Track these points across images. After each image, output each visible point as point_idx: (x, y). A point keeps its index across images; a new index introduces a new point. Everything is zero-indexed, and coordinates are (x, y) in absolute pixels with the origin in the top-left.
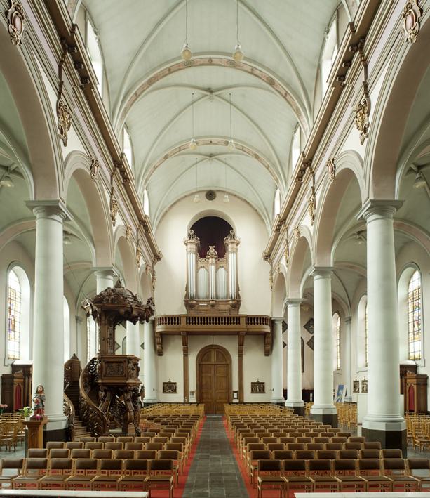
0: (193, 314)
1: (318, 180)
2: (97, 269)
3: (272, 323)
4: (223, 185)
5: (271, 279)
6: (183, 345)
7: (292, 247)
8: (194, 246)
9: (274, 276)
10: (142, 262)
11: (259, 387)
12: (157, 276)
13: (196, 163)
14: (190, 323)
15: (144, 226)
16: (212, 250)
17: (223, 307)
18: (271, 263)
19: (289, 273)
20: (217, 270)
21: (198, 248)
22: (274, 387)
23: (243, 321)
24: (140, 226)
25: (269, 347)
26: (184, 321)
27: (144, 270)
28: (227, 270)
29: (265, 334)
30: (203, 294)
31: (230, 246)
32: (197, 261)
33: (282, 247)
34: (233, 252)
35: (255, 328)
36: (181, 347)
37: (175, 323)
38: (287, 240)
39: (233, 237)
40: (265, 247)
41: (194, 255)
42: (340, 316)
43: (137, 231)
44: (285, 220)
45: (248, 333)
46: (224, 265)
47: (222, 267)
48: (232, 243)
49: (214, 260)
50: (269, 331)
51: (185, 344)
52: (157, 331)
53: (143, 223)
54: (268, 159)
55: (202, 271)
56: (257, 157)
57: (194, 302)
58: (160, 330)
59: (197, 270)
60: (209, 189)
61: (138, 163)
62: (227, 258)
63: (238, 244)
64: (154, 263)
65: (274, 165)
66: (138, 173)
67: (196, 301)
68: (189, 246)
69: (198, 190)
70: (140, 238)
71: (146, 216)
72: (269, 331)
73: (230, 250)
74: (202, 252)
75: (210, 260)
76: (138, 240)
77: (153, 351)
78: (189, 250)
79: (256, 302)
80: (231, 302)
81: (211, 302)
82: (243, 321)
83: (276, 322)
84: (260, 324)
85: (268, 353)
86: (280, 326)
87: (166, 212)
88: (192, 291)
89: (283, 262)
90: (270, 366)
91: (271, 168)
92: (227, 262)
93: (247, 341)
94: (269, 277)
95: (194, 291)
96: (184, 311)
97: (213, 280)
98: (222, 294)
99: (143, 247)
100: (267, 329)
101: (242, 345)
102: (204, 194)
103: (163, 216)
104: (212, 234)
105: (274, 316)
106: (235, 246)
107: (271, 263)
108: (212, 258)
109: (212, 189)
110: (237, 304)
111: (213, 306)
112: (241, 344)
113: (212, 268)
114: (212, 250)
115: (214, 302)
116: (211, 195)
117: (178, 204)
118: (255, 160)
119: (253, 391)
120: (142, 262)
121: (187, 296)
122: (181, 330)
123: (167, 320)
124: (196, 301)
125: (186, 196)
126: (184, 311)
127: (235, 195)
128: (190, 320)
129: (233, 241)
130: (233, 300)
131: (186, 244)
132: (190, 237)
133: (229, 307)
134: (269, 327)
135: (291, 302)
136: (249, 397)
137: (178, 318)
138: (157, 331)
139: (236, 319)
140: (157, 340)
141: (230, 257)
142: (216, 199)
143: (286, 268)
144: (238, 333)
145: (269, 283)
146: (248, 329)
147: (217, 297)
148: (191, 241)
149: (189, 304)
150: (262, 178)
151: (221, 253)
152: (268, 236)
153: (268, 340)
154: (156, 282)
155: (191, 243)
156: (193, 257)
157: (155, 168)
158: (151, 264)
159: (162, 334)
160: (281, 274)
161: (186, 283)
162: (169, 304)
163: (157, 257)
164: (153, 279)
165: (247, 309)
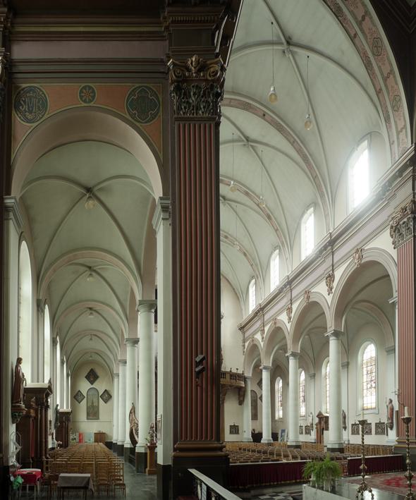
3: (245, 379)
11: (235, 430)
19: (265, 349)
22: (245, 429)
23: (228, 376)
25: (242, 399)
29: (242, 387)
56: (245, 255)
65: (256, 265)
82: (228, 376)
85: (241, 403)
90: (242, 414)
91: (254, 266)
118: (244, 257)
119: (231, 433)
136: (228, 437)
153: (242, 393)
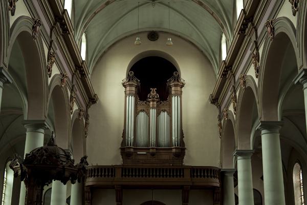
2: (28, 122)
3: (222, 175)
4: (166, 26)
6: (117, 201)
7: (224, 122)
8: (134, 89)
9: (222, 122)
10: (75, 108)
13: (139, 6)
15: (80, 72)
16: (153, 92)
17: (165, 156)
18: (219, 107)
20: (158, 114)
21: (138, 90)
23: (187, 173)
24: (75, 71)
26: (118, 173)
27: (77, 116)
28: (170, 114)
29: (215, 187)
31: (173, 88)
33: (229, 93)
34: (176, 95)
37: (108, 175)
38: (234, 87)
39: (178, 78)
40: (212, 90)
42: (301, 168)
43: (73, 76)
44: (231, 66)
45: (194, 187)
47: (164, 111)
48: (176, 86)
49: (155, 103)
50: (218, 185)
52: (87, 184)
53: (79, 68)
54: (212, 6)
55: (142, 115)
58: (90, 184)
59: (136, 113)
60: (151, 30)
61: (78, 11)
62: (171, 101)
63: (182, 86)
64: (88, 106)
65: (218, 12)
66: (77, 19)
68: (128, 88)
69: (140, 31)
70: (75, 83)
71: (83, 61)
72: (218, 185)
74: (141, 95)
75: (151, 103)
76: (73, 86)
78: (128, 92)
79: (203, 151)
80: (174, 150)
81: (151, 151)
82: (187, 173)
83: (226, 174)
84: (208, 176)
86: (231, 179)
87: (105, 52)
88: (131, 136)
89: (231, 108)
91: (215, 14)
94: (218, 122)
95: (132, 137)
96: (120, 162)
97: (156, 126)
99: (78, 93)
100: (216, 183)
102: (146, 35)
103: (101, 57)
104: (153, 79)
106: (179, 88)
107: (219, 107)
108: (153, 101)
109: (154, 30)
110: (181, 150)
111: (153, 154)
113: (153, 112)
114: (153, 92)
115: (155, 151)
116: (153, 36)
117: (118, 45)
120: (75, 108)
121: (124, 142)
123: (100, 171)
124: (134, 148)
125: (126, 37)
126: (120, 162)
127: (179, 36)
128: (125, 170)
129: (176, 83)
130: (175, 148)
132: (129, 78)
133: (172, 156)
134: (218, 181)
135: (241, 153)
137: (112, 169)
138: (87, 184)
139: (180, 170)
140: (87, 195)
141: (174, 100)
142: (158, 40)
143: (235, 116)
144: (181, 187)
145: (217, 129)
146: (193, 182)
147: (157, 143)
148: (130, 83)
149: (126, 150)
150: (209, 25)
151: (164, 96)
152: (216, 78)
155: (131, 85)
156: (131, 100)
157: (95, 14)
158: (84, 108)
159: (91, 187)
160: (229, 121)
161: (123, 128)
162: (103, 152)
163: (92, 99)
164: (86, 123)
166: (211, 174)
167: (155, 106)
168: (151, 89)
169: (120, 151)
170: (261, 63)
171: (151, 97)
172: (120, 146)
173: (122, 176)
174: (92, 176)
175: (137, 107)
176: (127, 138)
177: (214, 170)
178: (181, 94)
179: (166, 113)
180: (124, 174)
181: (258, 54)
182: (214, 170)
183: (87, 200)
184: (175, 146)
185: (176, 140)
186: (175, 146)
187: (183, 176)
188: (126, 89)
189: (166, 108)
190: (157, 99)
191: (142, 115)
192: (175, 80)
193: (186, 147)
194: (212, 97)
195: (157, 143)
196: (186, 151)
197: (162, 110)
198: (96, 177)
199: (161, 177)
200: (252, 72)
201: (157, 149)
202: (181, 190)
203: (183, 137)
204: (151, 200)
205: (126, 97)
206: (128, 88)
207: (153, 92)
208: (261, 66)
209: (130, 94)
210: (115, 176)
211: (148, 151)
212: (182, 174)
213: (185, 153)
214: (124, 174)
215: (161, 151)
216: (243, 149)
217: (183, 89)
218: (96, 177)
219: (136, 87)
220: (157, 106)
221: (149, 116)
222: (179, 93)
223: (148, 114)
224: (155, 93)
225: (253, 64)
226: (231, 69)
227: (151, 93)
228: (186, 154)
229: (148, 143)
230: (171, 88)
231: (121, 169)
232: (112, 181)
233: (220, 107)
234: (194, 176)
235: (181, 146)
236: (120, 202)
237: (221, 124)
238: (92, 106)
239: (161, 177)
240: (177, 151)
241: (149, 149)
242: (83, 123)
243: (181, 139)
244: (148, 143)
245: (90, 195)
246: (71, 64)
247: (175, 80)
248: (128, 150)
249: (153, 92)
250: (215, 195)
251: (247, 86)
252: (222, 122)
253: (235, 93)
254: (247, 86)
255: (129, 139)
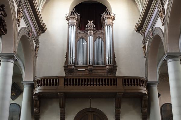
0: (71, 76)
1: (146, 36)
3: (149, 86)
5: (144, 47)
6: (61, 108)
8: (75, 21)
9: (147, 44)
12: (40, 45)
14: (67, 85)
16: (91, 24)
20: (94, 40)
21: (79, 22)
23: (120, 82)
26: (62, 82)
28: (104, 40)
30: (81, 60)
31: (106, 21)
32: (77, 33)
35: (131, 89)
36: (59, 110)
40: (137, 20)
41: (75, 28)
46: (101, 36)
47: (99, 38)
48: (108, 18)
49: (92, 31)
50: (146, 92)
51: (62, 107)
57: (73, 67)
59: (77, 40)
62: (104, 30)
63: (113, 19)
64: (38, 34)
67: (75, 66)
72: (146, 92)
73: (106, 24)
74: (82, 26)
75: (89, 31)
77: (31, 115)
80: (108, 67)
81: (89, 68)
82: (120, 82)
83: (151, 86)
84: (137, 85)
88: (72, 57)
92: (104, 34)
93: (124, 106)
94: (142, 46)
95: (74, 58)
97: (92, 49)
98: (99, 60)
101: (120, 108)
105: (150, 80)
106: (111, 20)
108: (90, 30)
110: (114, 66)
111: (90, 71)
112: (118, 107)
113: (90, 39)
114: (91, 24)
115: (92, 68)
121: (67, 62)
122: (58, 91)
128: (67, 81)
129: (108, 16)
130: (108, 65)
131: (68, 19)
134: (145, 89)
139: (114, 80)
140: (35, 103)
141: (107, 29)
145: (142, 52)
147: (94, 62)
148: (72, 16)
149: (67, 67)
151: (99, 26)
153: (145, 103)
154: (39, 51)
155: (73, 18)
156: (73, 30)
161: (66, 51)
163: (42, 28)
164: (36, 46)
165: (123, 71)
166: (140, 83)
167: (92, 34)
168: (89, 21)
169: (64, 68)
170: (166, 15)
171: (88, 27)
172: (64, 65)
173: (65, 85)
174: (39, 86)
175: (77, 35)
176: (69, 58)
177: (142, 80)
178: (113, 25)
179: (100, 39)
180: (66, 83)
181: (163, 9)
182: (142, 80)
183: (35, 107)
184: (109, 63)
185: (109, 59)
186: (109, 63)
187: (116, 85)
188: (68, 22)
189: (100, 36)
190: (93, 28)
191: (82, 42)
192: (107, 14)
193: (117, 65)
194: (138, 25)
195: (94, 62)
196: (117, 68)
197: (98, 37)
198: (42, 86)
199: (98, 86)
200: (159, 23)
201: (93, 66)
202: (114, 99)
203: (115, 57)
204: (90, 107)
205: (69, 27)
206: (70, 21)
207: (91, 23)
208: (166, 17)
209: (72, 25)
210: (58, 85)
211: (86, 68)
212: (115, 83)
213: (116, 69)
214: (66, 83)
215: (97, 68)
216: (173, 52)
217: (114, 22)
218: (42, 86)
219: (77, 20)
220: (94, 34)
221: (87, 42)
222: (111, 24)
223: (86, 41)
224: (92, 24)
225: (159, 18)
226: (142, 29)
227: (89, 24)
228: (117, 70)
229: (87, 62)
230: (104, 20)
231: (63, 80)
232: (56, 89)
233: (144, 34)
234: (125, 85)
235: (113, 64)
236: (63, 108)
237: (145, 46)
238: (42, 35)
239: (98, 86)
240: (110, 67)
241: (87, 67)
242: (33, 46)
243: (113, 58)
244: (87, 62)
245: (38, 102)
246: (30, 10)
247: (107, 14)
248: (70, 67)
249: (91, 23)
250: (143, 102)
251: (154, 35)
252: (147, 44)
253: (163, 6)
254: (154, 35)
255: (71, 59)
